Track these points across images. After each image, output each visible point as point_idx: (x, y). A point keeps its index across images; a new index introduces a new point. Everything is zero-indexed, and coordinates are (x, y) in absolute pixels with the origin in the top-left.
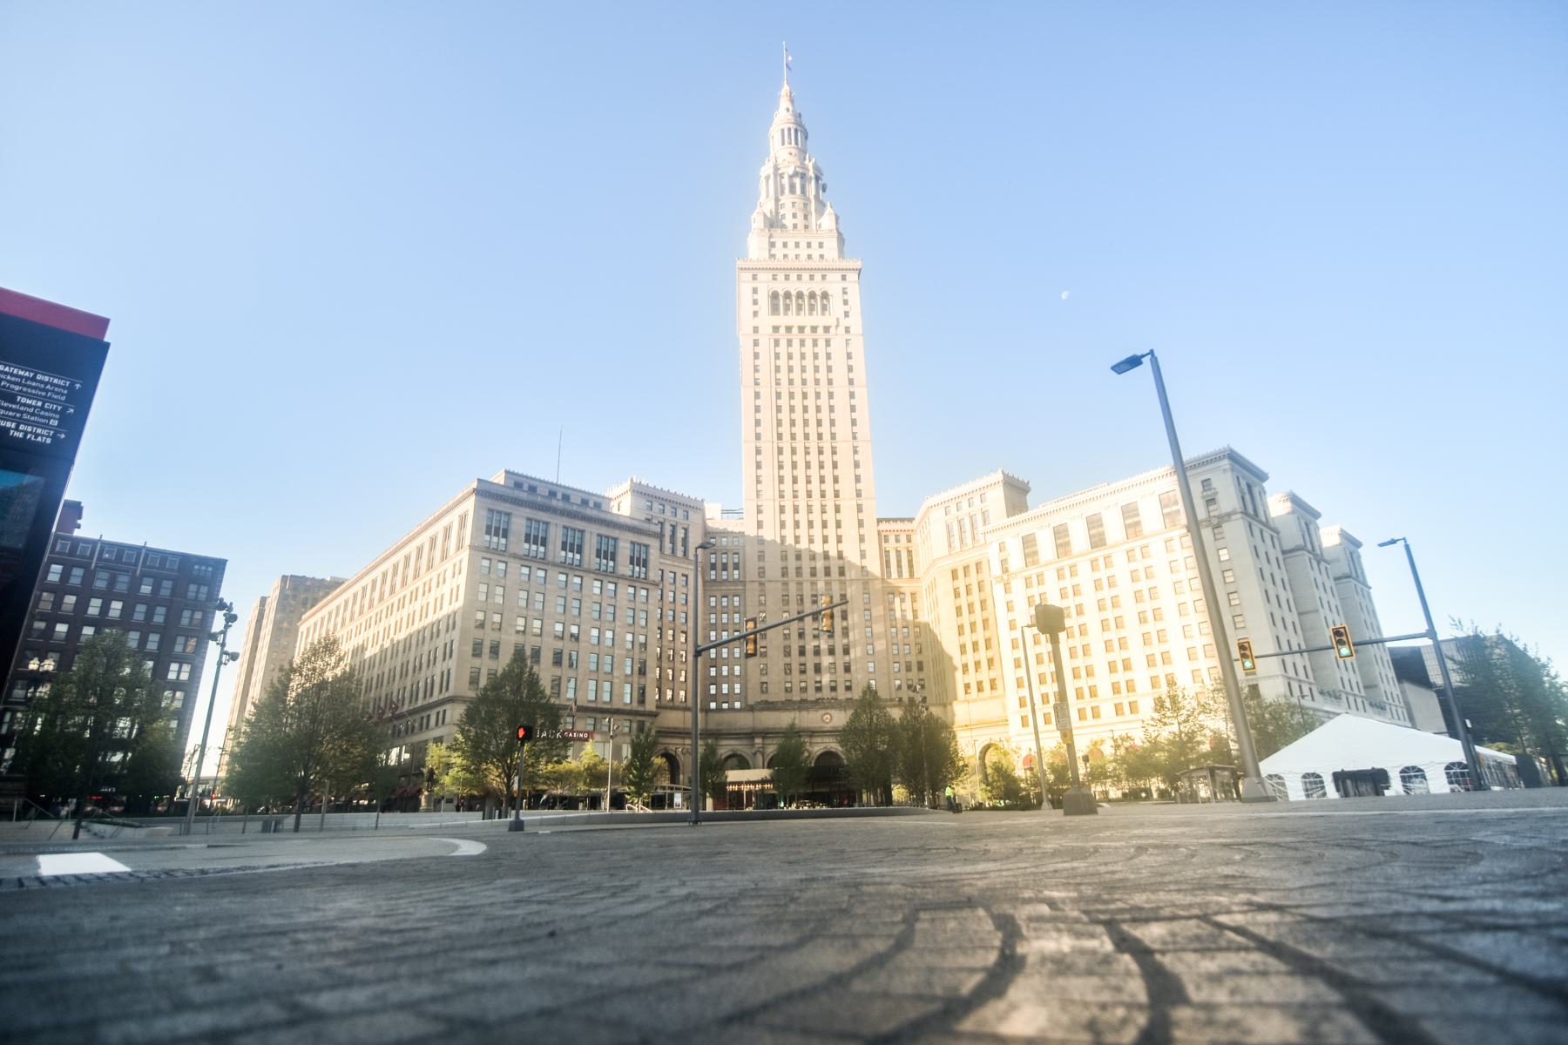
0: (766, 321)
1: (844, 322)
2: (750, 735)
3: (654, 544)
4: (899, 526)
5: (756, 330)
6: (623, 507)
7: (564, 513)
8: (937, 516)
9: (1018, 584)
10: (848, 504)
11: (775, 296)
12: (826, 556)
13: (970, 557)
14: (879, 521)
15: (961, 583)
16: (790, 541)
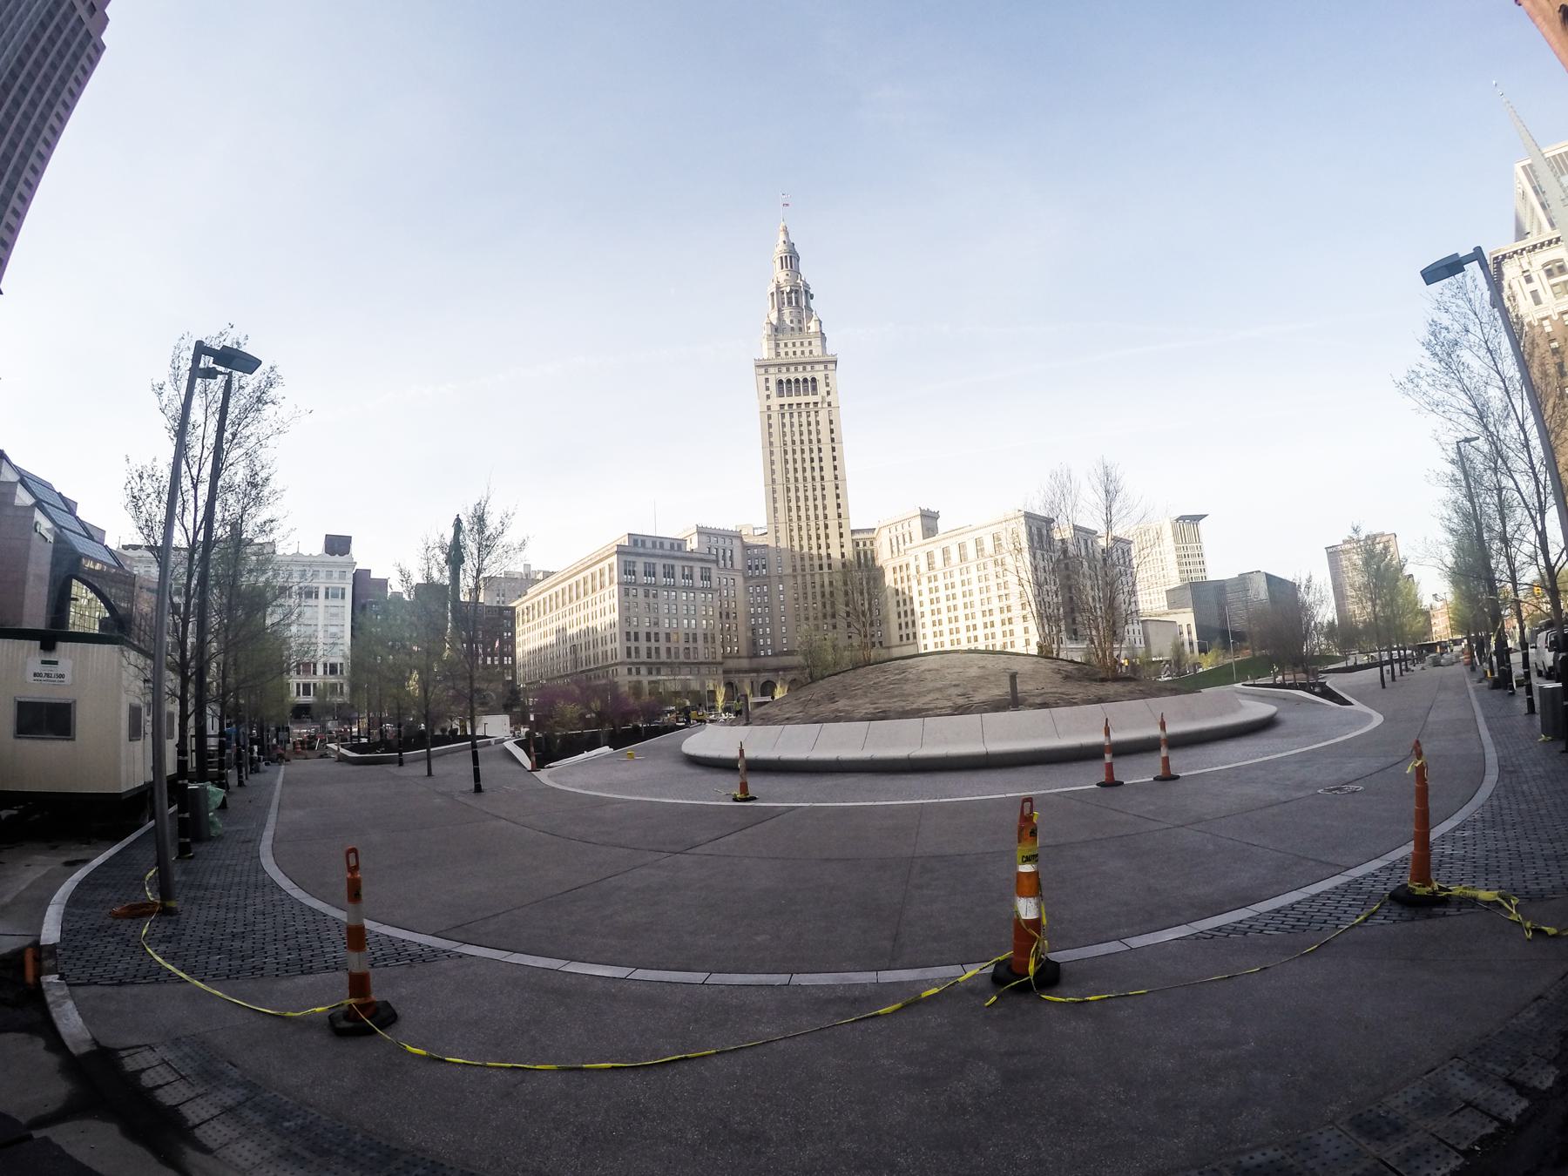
0: (775, 402)
1: (828, 399)
2: (776, 670)
3: (713, 566)
4: (865, 536)
5: (769, 408)
6: (693, 544)
7: (663, 556)
8: (885, 532)
9: (924, 580)
10: (833, 523)
11: (780, 382)
12: (820, 557)
13: (902, 561)
14: (853, 532)
15: (898, 576)
16: (797, 548)
